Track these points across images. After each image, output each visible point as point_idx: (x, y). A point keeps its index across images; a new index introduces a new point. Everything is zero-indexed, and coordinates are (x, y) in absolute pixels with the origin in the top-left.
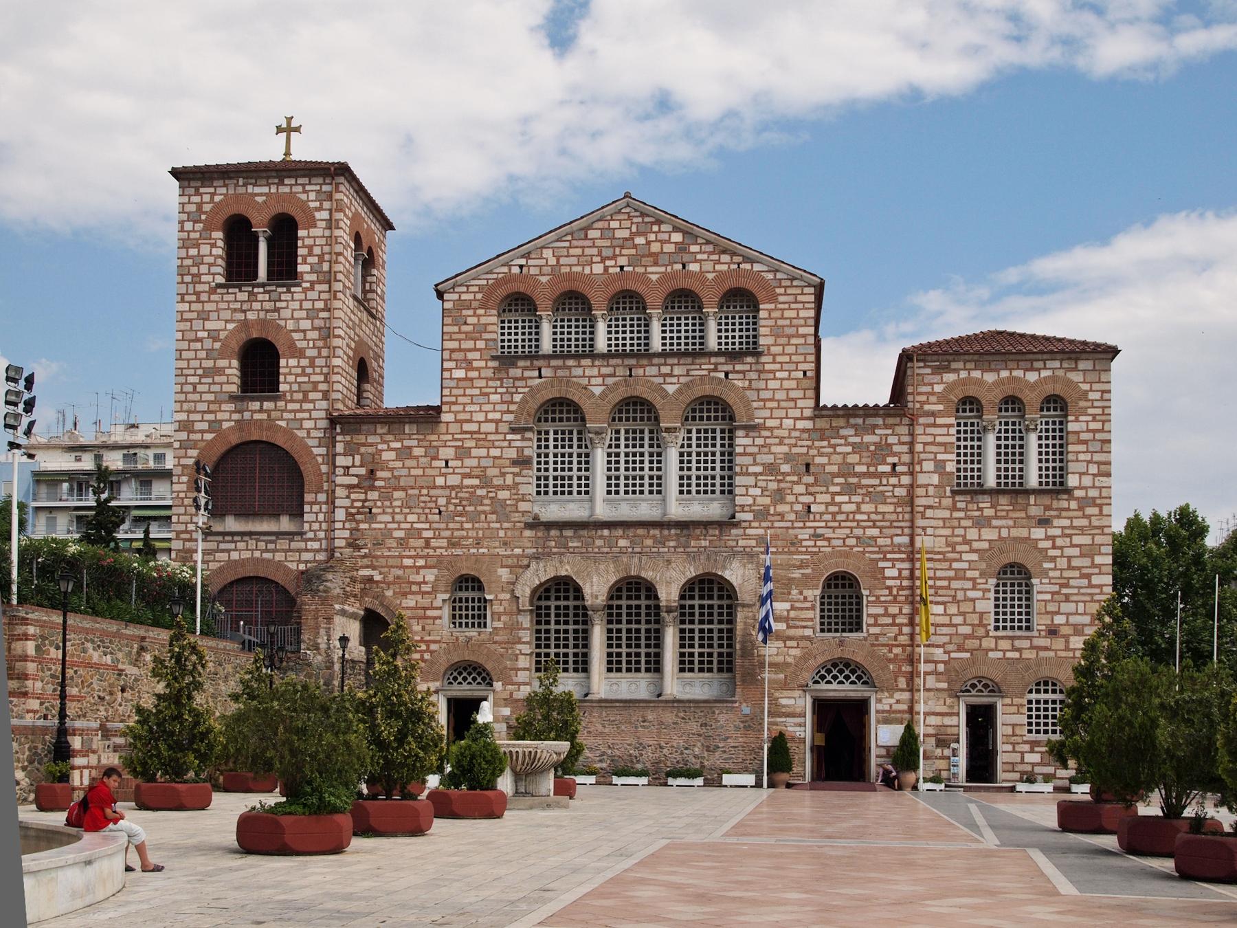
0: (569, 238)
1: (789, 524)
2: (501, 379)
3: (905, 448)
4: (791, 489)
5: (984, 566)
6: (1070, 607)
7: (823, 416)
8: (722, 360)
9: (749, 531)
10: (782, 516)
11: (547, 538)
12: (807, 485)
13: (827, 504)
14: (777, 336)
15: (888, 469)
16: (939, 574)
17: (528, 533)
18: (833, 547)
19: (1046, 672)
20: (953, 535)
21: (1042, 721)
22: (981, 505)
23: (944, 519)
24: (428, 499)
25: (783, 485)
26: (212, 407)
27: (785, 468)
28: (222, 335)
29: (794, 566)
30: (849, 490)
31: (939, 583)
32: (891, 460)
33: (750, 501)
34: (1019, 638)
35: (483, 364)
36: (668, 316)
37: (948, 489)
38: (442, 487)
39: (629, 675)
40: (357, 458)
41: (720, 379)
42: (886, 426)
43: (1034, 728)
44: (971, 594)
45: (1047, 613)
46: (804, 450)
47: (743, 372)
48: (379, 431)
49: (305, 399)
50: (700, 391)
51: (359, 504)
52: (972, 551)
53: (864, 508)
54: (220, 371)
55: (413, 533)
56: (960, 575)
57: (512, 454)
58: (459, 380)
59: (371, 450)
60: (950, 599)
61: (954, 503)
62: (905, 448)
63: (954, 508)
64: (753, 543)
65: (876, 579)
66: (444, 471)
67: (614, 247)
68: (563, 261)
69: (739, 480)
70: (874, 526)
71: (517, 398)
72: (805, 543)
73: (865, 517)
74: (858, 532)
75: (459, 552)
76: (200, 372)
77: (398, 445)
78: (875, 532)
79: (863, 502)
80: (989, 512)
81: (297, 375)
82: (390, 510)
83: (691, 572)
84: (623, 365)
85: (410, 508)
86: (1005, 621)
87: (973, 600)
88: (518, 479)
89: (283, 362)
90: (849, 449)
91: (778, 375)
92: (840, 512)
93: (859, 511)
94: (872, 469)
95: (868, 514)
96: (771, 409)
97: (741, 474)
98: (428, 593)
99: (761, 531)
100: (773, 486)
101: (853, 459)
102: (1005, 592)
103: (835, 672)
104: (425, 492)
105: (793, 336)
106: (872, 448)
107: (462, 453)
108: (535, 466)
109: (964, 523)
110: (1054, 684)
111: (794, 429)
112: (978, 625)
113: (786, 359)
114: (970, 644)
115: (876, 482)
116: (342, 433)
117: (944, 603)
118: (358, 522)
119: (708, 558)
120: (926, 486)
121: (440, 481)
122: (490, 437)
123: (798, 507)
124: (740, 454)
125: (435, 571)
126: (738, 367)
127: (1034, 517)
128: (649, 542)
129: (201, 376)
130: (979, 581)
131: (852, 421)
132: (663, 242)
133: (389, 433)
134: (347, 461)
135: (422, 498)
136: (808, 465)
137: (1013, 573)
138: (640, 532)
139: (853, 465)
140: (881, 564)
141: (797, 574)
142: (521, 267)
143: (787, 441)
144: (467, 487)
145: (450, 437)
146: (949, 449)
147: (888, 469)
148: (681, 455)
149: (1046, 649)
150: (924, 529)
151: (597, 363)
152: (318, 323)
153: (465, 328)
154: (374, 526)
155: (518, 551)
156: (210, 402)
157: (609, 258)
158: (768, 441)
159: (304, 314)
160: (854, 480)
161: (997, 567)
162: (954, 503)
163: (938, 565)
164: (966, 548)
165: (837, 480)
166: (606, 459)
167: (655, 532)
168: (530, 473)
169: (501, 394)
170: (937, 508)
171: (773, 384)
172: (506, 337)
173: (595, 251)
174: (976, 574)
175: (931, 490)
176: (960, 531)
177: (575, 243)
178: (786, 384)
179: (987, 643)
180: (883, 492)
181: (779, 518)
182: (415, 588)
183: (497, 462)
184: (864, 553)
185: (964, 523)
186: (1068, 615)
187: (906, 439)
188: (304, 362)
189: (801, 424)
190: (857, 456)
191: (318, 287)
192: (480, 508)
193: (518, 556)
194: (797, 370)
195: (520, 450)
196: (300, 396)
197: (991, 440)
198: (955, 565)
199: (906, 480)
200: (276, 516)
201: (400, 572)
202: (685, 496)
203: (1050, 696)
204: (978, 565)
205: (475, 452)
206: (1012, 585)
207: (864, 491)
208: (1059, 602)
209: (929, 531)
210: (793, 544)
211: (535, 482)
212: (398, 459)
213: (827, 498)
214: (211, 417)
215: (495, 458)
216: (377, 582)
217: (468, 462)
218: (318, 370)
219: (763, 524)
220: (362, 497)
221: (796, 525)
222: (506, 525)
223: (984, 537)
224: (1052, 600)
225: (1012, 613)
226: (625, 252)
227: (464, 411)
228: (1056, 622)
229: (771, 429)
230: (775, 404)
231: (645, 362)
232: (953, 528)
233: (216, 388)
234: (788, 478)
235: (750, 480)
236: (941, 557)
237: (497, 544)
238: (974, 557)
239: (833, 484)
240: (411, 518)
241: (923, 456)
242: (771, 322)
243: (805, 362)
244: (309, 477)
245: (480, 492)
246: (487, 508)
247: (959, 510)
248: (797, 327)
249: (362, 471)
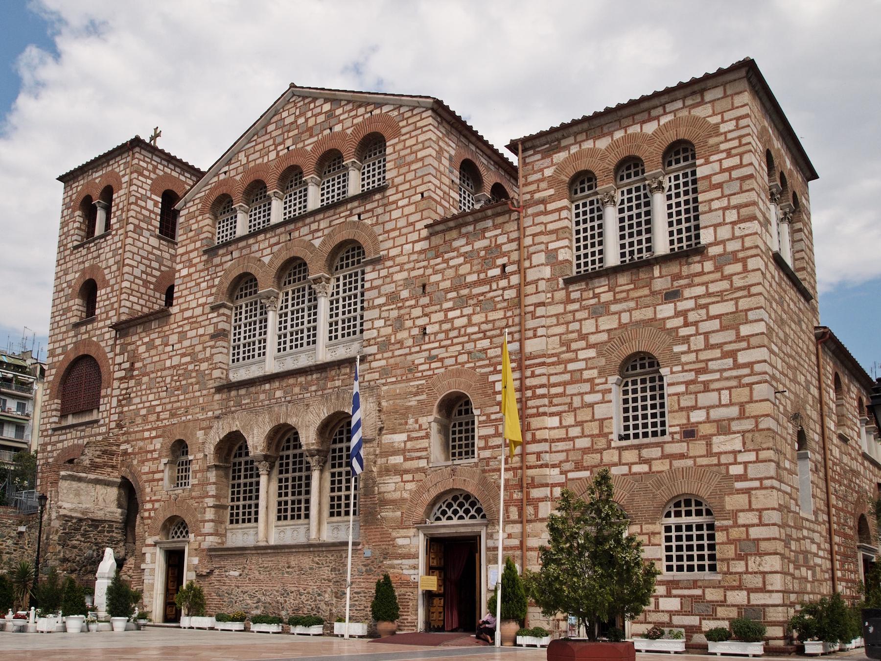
0: (255, 138)
1: (407, 351)
2: (208, 269)
3: (514, 245)
4: (409, 314)
5: (602, 362)
6: (710, 398)
7: (437, 233)
8: (356, 204)
9: (374, 364)
10: (401, 342)
11: (228, 399)
12: (423, 307)
13: (441, 322)
14: (398, 167)
15: (497, 272)
16: (553, 380)
17: (217, 397)
18: (446, 367)
19: (684, 488)
20: (568, 332)
21: (685, 553)
22: (597, 291)
23: (557, 315)
24: (160, 379)
25: (402, 312)
26: (65, 336)
27: (405, 294)
28: (73, 282)
29: (411, 393)
30: (461, 303)
31: (554, 391)
32: (500, 262)
33: (374, 333)
34: (647, 446)
35: (198, 260)
36: (326, 180)
37: (560, 280)
38: (169, 368)
39: (292, 522)
40: (126, 354)
41: (354, 222)
42: (495, 227)
43: (674, 563)
44: (589, 398)
45: (681, 409)
46: (421, 271)
47: (372, 210)
48: (139, 331)
49: (108, 318)
50: (338, 239)
51: (124, 392)
52: (589, 346)
53: (476, 319)
54: (69, 309)
55: (151, 409)
56: (576, 378)
57: (211, 330)
58: (184, 277)
59: (133, 347)
60: (566, 408)
61: (568, 294)
62: (514, 245)
63: (568, 301)
64: (376, 375)
65: (487, 395)
66: (171, 354)
67: (283, 133)
68: (251, 158)
69: (367, 315)
70: (485, 337)
71: (217, 281)
72: (421, 368)
73: (476, 329)
74: (469, 346)
75: (175, 421)
76: (61, 312)
77: (146, 340)
78: (486, 343)
79: (474, 314)
80: (607, 297)
81: (104, 301)
82: (139, 393)
83: (324, 414)
84: (285, 232)
85: (150, 389)
86: (636, 427)
87: (591, 405)
88: (214, 351)
89: (98, 294)
90: (461, 260)
91: (400, 203)
92: (453, 329)
93: (470, 324)
94: (482, 276)
95: (479, 325)
96: (394, 238)
97: (369, 308)
98: (156, 459)
99: (383, 363)
100: (394, 314)
101: (465, 269)
102: (635, 391)
103: (455, 507)
104: (159, 374)
105: (412, 162)
106: (482, 253)
107: (183, 336)
108: (232, 338)
109: (579, 315)
110: (698, 503)
111: (413, 253)
112: (598, 436)
113: (407, 186)
114: (592, 459)
115: (486, 288)
116: (120, 338)
117: (559, 414)
118: (123, 406)
119: (338, 398)
120: (536, 282)
121: (168, 363)
122: (200, 319)
123: (415, 331)
124: (368, 289)
125: (161, 439)
126: (368, 207)
127: (659, 292)
128: (297, 390)
129: (61, 315)
130: (597, 381)
131: (464, 230)
132: (316, 116)
133: (144, 331)
134: (119, 359)
135: (158, 380)
136: (424, 286)
137: (643, 366)
138: (291, 381)
139: (464, 276)
140: (492, 378)
141: (413, 402)
142: (225, 173)
143: (406, 267)
144: (183, 364)
145: (175, 325)
146: (561, 235)
147: (497, 272)
148: (332, 303)
149: (682, 456)
150: (535, 330)
151: (268, 236)
152: (118, 258)
153: (191, 234)
154: (132, 408)
155: (210, 414)
156: (64, 332)
157: (280, 144)
158: (391, 270)
159: (111, 254)
160: (465, 292)
161: (617, 358)
162: (568, 294)
163: (552, 370)
164: (582, 344)
165: (451, 295)
166: (278, 319)
167: (301, 379)
168: (225, 344)
169: (207, 281)
170: (550, 304)
171: (396, 214)
172: (221, 234)
173: (271, 142)
174: (594, 373)
175: (542, 285)
176: (575, 326)
177: (259, 140)
178: (407, 211)
179: (610, 456)
180: (492, 298)
181: (398, 346)
182: (149, 456)
183: (203, 338)
184: (474, 368)
185: (579, 315)
186: (708, 408)
187: (514, 235)
188: (109, 290)
189: (418, 247)
190: (468, 266)
191: (120, 232)
192: (190, 381)
193: (209, 419)
194: (416, 194)
195: (216, 324)
196: (104, 316)
197: (611, 215)
198: (571, 367)
199: (515, 280)
200: (91, 411)
201: (141, 444)
202: (334, 341)
203: (694, 519)
204: (596, 362)
205: (191, 334)
206: (643, 381)
207: (475, 301)
208: (696, 393)
209: (540, 332)
210: (410, 371)
211: (231, 351)
212: (148, 351)
213: (440, 316)
214: (63, 343)
215: (201, 336)
216: (130, 454)
217: (186, 343)
218: (115, 293)
219: (386, 355)
220: (125, 385)
221: (414, 350)
222: (205, 392)
223: (601, 328)
224: (687, 392)
225: (645, 417)
226: (291, 134)
227: (186, 302)
228: (693, 420)
229: (393, 258)
230: (397, 233)
231: (300, 224)
232: (568, 323)
233: (67, 322)
234: (407, 304)
235: (375, 313)
236: (555, 359)
237: (198, 410)
238: (592, 353)
239: (447, 300)
240: (151, 397)
241: (532, 249)
242: (395, 156)
243: (423, 183)
244: (105, 377)
245: (191, 367)
246: (193, 380)
247: (574, 301)
248: (416, 152)
249: (127, 365)
